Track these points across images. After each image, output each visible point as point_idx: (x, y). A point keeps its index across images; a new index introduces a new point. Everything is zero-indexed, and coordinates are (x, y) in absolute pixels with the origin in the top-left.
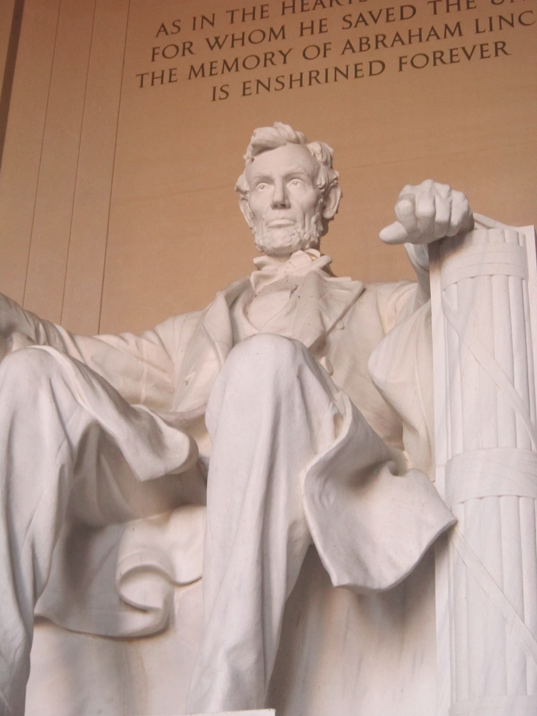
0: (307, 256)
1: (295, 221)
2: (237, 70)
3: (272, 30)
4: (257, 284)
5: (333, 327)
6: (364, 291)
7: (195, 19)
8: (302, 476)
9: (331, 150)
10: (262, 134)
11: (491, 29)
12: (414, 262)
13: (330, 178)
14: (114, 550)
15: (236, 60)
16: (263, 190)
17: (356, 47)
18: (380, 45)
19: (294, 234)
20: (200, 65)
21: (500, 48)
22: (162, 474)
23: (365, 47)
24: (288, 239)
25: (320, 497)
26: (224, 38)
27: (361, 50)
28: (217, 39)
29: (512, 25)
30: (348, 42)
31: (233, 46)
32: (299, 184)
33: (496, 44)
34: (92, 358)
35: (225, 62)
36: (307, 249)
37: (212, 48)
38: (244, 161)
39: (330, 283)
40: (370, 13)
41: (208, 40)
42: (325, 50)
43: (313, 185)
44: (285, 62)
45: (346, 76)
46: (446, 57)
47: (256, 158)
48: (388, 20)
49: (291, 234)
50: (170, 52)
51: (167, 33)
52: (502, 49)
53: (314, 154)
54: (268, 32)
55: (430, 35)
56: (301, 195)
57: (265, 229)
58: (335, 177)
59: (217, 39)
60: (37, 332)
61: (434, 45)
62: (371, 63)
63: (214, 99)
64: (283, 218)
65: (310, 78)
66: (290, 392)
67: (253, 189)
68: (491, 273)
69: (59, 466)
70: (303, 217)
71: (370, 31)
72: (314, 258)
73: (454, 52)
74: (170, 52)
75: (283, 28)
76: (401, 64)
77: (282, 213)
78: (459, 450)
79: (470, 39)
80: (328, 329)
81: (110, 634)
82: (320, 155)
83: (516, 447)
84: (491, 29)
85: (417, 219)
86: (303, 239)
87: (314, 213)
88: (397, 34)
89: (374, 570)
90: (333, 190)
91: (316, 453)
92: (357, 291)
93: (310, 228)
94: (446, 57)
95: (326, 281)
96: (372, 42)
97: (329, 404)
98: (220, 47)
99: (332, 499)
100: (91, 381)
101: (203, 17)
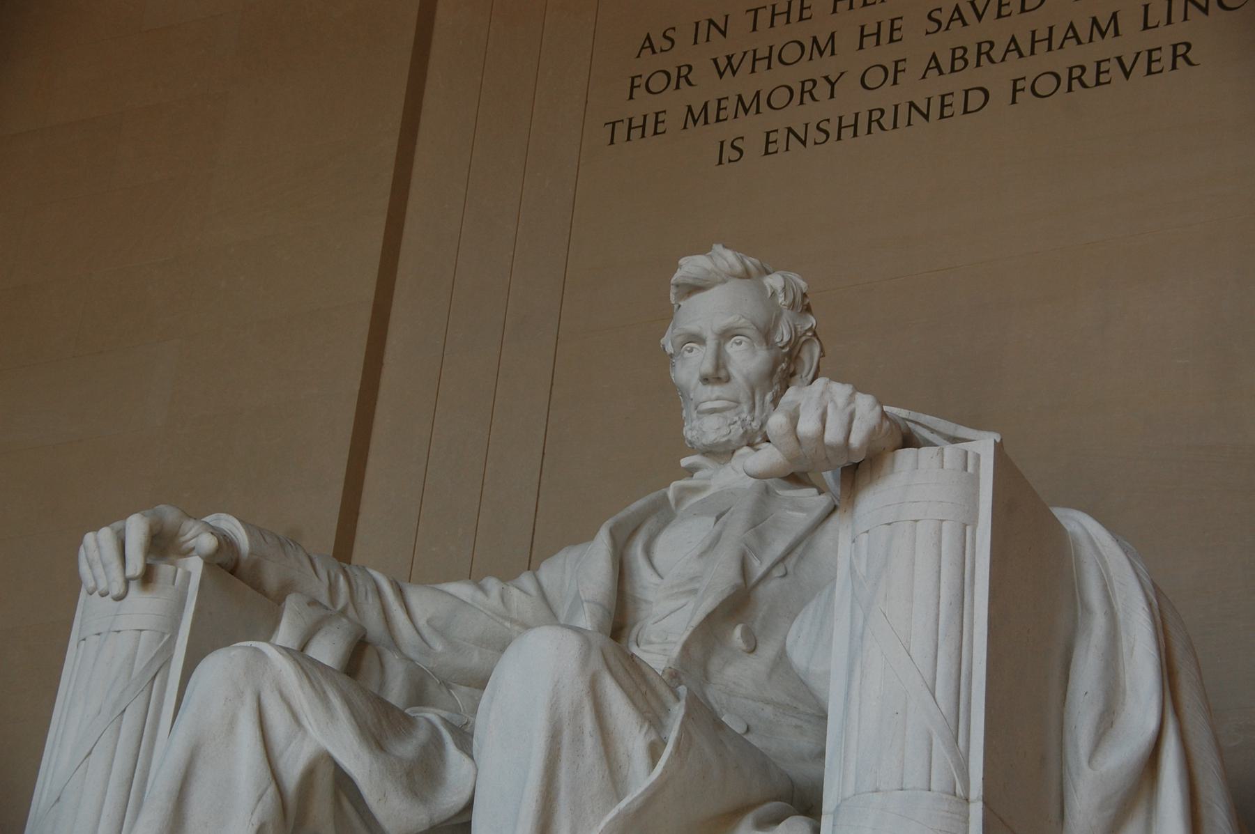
1: (738, 402)
2: (758, 112)
3: (815, 40)
4: (679, 501)
5: (766, 575)
7: (697, 24)
9: (803, 284)
11: (1169, 22)
15: (758, 94)
17: (946, 65)
21: (1181, 54)
22: (427, 827)
23: (959, 64)
24: (724, 431)
27: (953, 70)
28: (729, 58)
30: (934, 57)
31: (753, 71)
33: (1175, 47)
34: (428, 622)
35: (740, 98)
37: (721, 75)
41: (715, 61)
44: (832, 96)
45: (926, 117)
46: (1089, 78)
48: (999, 16)
50: (658, 82)
51: (654, 52)
52: (1184, 56)
54: (808, 44)
55: (1066, 38)
56: (746, 360)
57: (694, 415)
59: (729, 58)
60: (333, 589)
62: (967, 92)
63: (720, 163)
64: (718, 399)
65: (870, 121)
66: (576, 713)
69: (256, 827)
73: (1104, 67)
74: (658, 82)
75: (832, 36)
76: (1015, 91)
77: (717, 390)
78: (849, 791)
79: (1132, 40)
80: (754, 580)
82: (782, 295)
84: (1169, 22)
88: (1013, 40)
90: (806, 348)
91: (620, 800)
92: (817, 512)
93: (763, 410)
94: (1089, 78)
96: (972, 57)
98: (734, 73)
101: (711, 22)
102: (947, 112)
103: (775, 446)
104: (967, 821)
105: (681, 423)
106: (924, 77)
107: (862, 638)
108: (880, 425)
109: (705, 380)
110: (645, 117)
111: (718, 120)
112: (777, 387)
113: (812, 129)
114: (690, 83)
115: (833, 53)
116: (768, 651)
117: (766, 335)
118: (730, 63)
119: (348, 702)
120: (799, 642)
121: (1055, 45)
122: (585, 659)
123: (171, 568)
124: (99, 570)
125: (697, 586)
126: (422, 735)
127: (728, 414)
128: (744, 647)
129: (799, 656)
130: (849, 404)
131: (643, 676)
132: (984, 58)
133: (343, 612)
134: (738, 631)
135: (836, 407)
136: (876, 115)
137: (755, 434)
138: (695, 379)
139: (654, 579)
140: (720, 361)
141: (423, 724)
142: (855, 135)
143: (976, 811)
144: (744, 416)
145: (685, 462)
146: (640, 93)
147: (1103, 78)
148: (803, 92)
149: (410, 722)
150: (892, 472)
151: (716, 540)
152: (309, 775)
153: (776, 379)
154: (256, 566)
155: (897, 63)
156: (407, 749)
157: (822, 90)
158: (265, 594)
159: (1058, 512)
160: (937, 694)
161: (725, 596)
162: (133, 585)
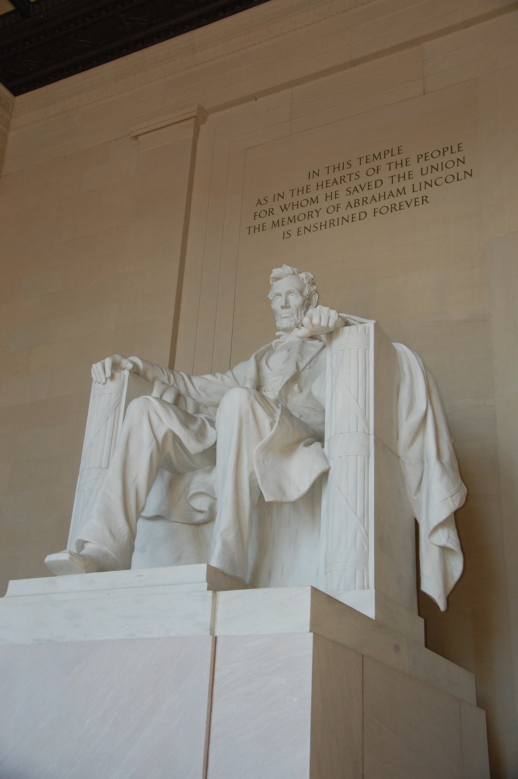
3: (312, 199)
4: (275, 347)
6: (325, 346)
9: (312, 276)
11: (420, 190)
14: (189, 484)
17: (353, 206)
21: (425, 199)
23: (357, 205)
25: (263, 461)
28: (285, 205)
29: (431, 186)
30: (349, 203)
33: (423, 197)
35: (289, 218)
37: (283, 211)
40: (360, 185)
45: (348, 221)
46: (397, 207)
50: (263, 214)
52: (425, 200)
54: (310, 200)
56: (295, 301)
57: (279, 319)
59: (285, 205)
60: (169, 379)
61: (392, 201)
71: (359, 196)
73: (402, 204)
75: (317, 197)
76: (375, 212)
78: (333, 434)
79: (410, 196)
80: (300, 370)
81: (189, 522)
84: (420, 190)
87: (303, 309)
94: (397, 207)
98: (287, 210)
102: (354, 220)
104: (369, 441)
105: (275, 321)
108: (338, 320)
109: (282, 308)
112: (305, 309)
113: (312, 226)
116: (306, 392)
117: (301, 292)
119: (176, 413)
120: (316, 389)
121: (386, 198)
123: (119, 374)
124: (98, 376)
126: (199, 422)
127: (290, 318)
128: (298, 391)
129: (316, 393)
131: (267, 402)
132: (364, 202)
133: (173, 386)
134: (296, 386)
136: (332, 221)
138: (279, 308)
139: (270, 371)
140: (287, 302)
141: (199, 419)
143: (372, 437)
145: (277, 334)
146: (257, 218)
147: (402, 207)
149: (196, 419)
152: (166, 435)
153: (304, 306)
154: (145, 372)
156: (195, 427)
157: (315, 214)
158: (148, 381)
159: (394, 344)
160: (359, 402)
162: (108, 379)
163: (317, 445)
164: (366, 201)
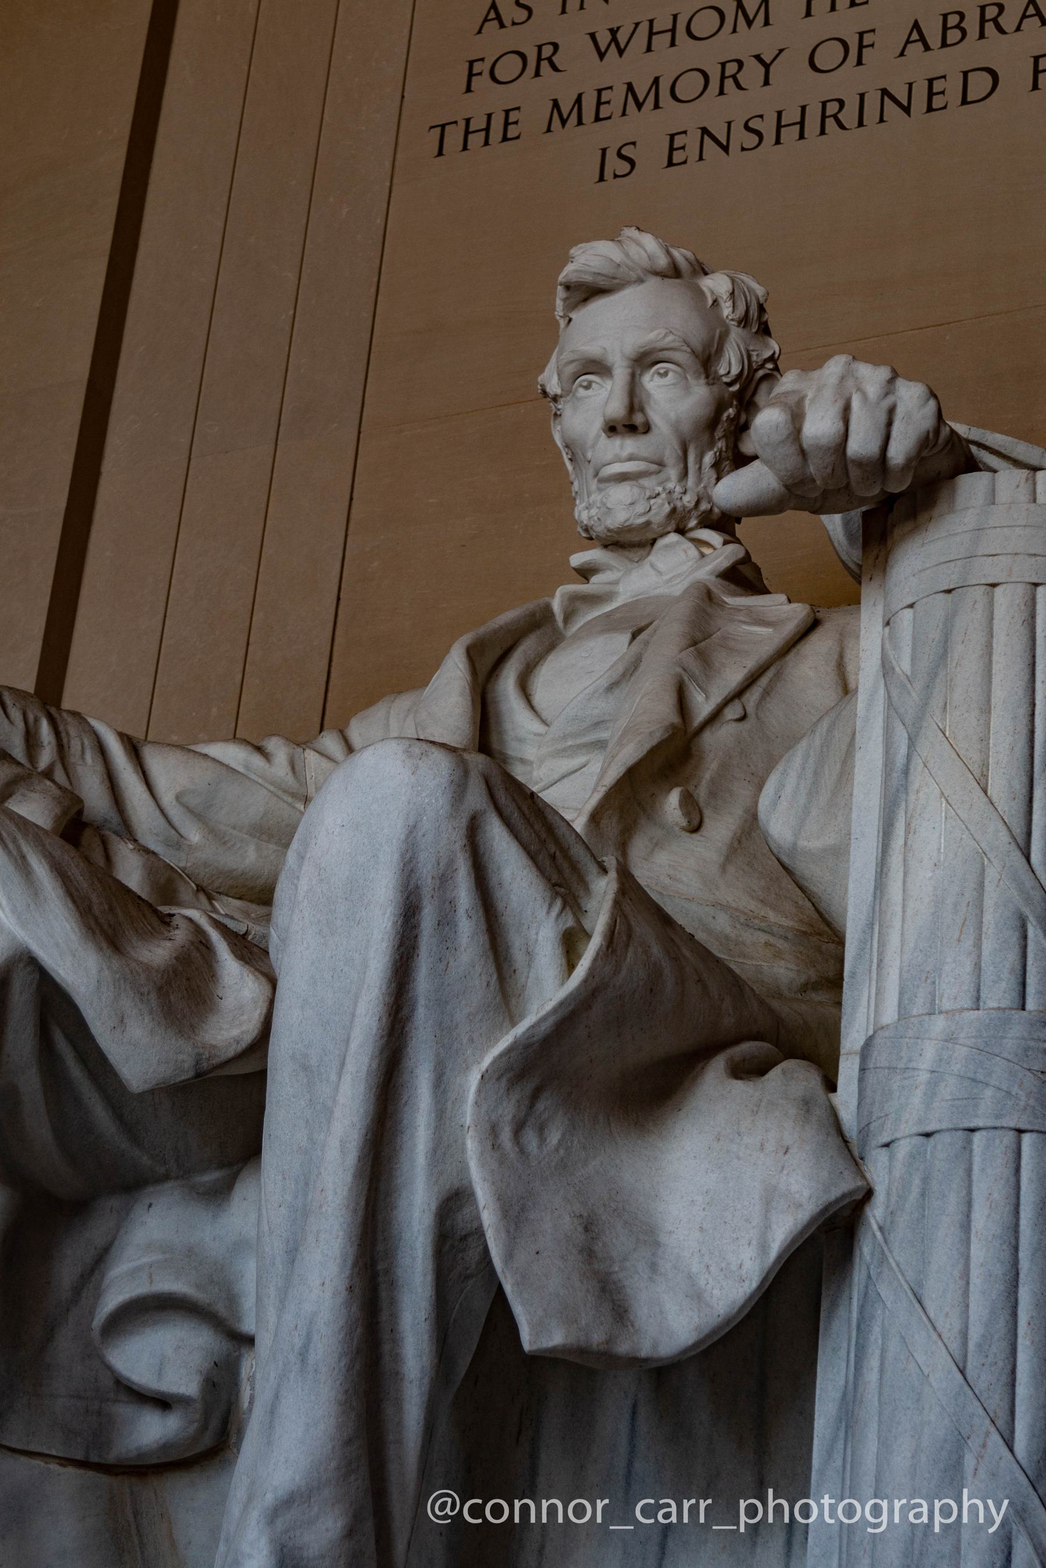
0: (690, 545)
1: (661, 464)
2: (657, 106)
4: (568, 617)
5: (715, 716)
8: (474, 1080)
10: (590, 258)
12: (845, 558)
13: (754, 358)
14: (101, 1259)
15: (656, 81)
16: (589, 392)
17: (934, 39)
18: (990, 27)
19: (659, 494)
20: (575, 97)
23: (953, 36)
24: (640, 508)
26: (632, 28)
27: (944, 44)
28: (613, 32)
30: (916, 26)
31: (649, 49)
32: (670, 374)
34: (178, 798)
35: (630, 87)
36: (692, 529)
37: (602, 56)
38: (557, 322)
39: (738, 609)
41: (593, 36)
42: (861, 47)
43: (707, 377)
44: (766, 82)
45: (907, 110)
47: (573, 315)
49: (648, 494)
50: (509, 67)
51: (502, 26)
53: (715, 301)
56: (675, 400)
57: (594, 485)
58: (767, 354)
59: (613, 32)
60: (31, 740)
62: (965, 74)
63: (602, 179)
64: (631, 458)
66: (445, 879)
67: (568, 392)
68: (991, 581)
70: (680, 452)
72: (707, 551)
74: (509, 67)
77: (629, 445)
78: (890, 1015)
82: (729, 303)
83: (1023, 1009)
85: (803, 452)
86: (679, 504)
87: (712, 444)
89: (642, 1312)
91: (514, 1024)
92: (790, 628)
93: (700, 479)
95: (722, 605)
96: (972, 24)
97: (550, 906)
98: (621, 52)
99: (554, 1137)
100: (23, 857)
103: (766, 462)
106: (902, 54)
107: (906, 772)
108: (937, 431)
110: (489, 116)
111: (598, 119)
112: (721, 444)
114: (555, 69)
115: (767, 23)
116: (721, 828)
117: (706, 361)
118: (614, 39)
122: (459, 790)
125: (604, 735)
126: (181, 935)
127: (645, 482)
128: (683, 822)
129: (779, 825)
130: (887, 394)
132: (990, 27)
133: (48, 774)
134: (674, 798)
135: (865, 396)
137: (686, 514)
138: (598, 424)
139: (536, 726)
140: (635, 402)
142: (802, 136)
144: (670, 485)
146: (481, 83)
148: (723, 78)
150: (952, 510)
151: (632, 668)
153: (719, 433)
155: (861, 35)
156: (158, 953)
161: (655, 741)
163: (792, 1079)
164: (995, 20)
